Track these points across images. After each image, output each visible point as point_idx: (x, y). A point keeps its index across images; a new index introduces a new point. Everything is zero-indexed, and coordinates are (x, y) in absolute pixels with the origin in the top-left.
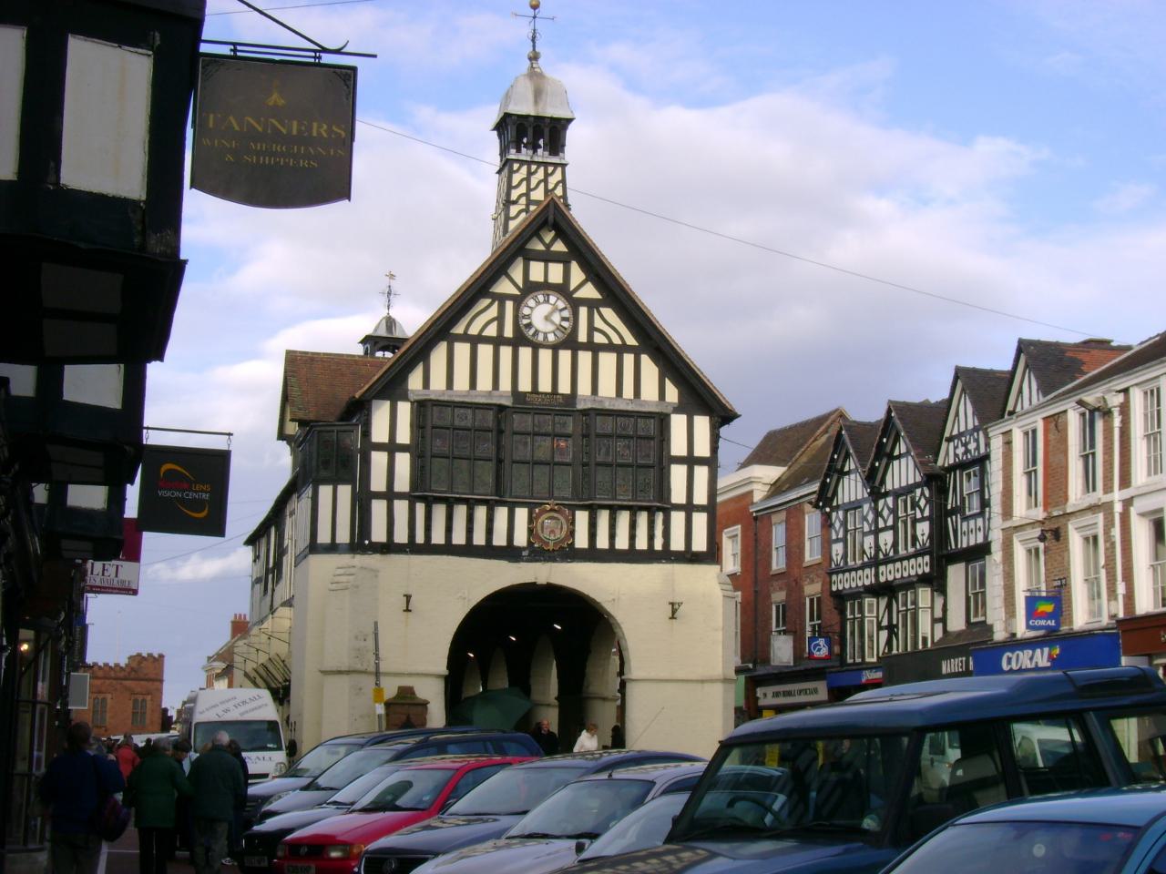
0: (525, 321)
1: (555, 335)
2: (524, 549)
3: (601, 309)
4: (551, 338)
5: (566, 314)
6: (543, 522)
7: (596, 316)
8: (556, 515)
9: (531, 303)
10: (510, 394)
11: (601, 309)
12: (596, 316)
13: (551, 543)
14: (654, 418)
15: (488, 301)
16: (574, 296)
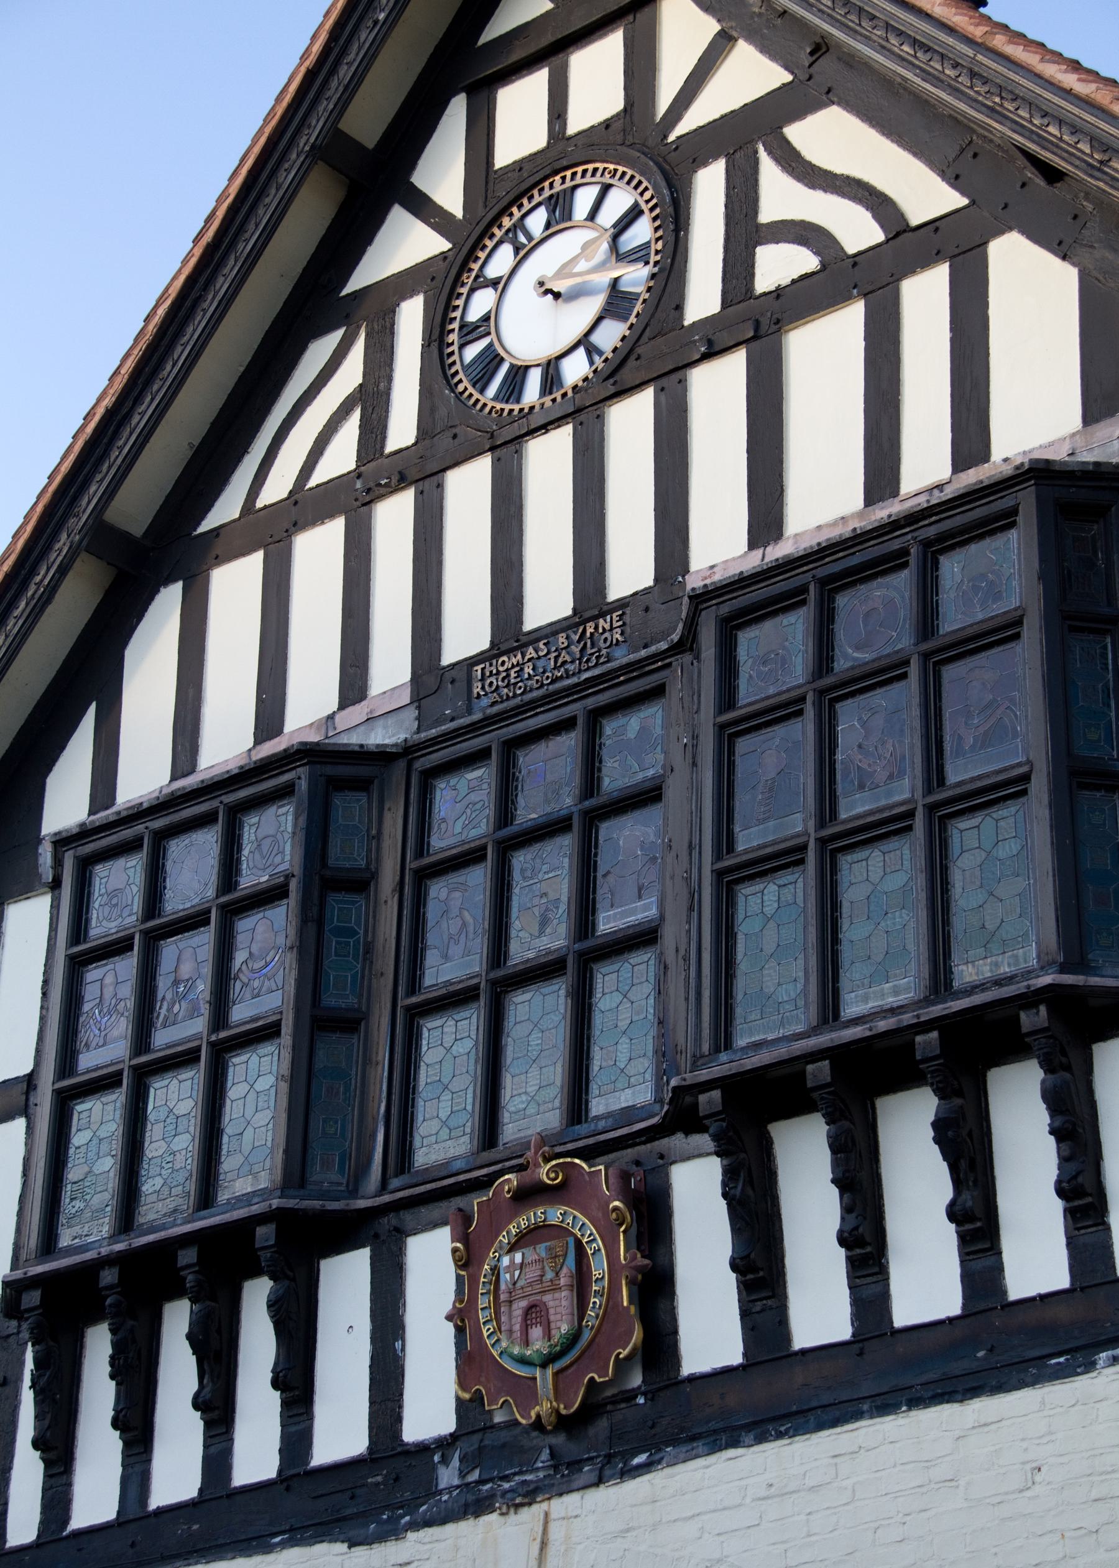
0: (472, 352)
1: (592, 351)
2: (444, 1444)
3: (795, 133)
4: (576, 369)
5: (642, 232)
6: (495, 1270)
7: (770, 173)
8: (555, 1214)
9: (501, 262)
10: (405, 698)
11: (795, 133)
12: (770, 173)
13: (544, 1379)
14: (1005, 521)
15: (333, 339)
16: (672, 138)
